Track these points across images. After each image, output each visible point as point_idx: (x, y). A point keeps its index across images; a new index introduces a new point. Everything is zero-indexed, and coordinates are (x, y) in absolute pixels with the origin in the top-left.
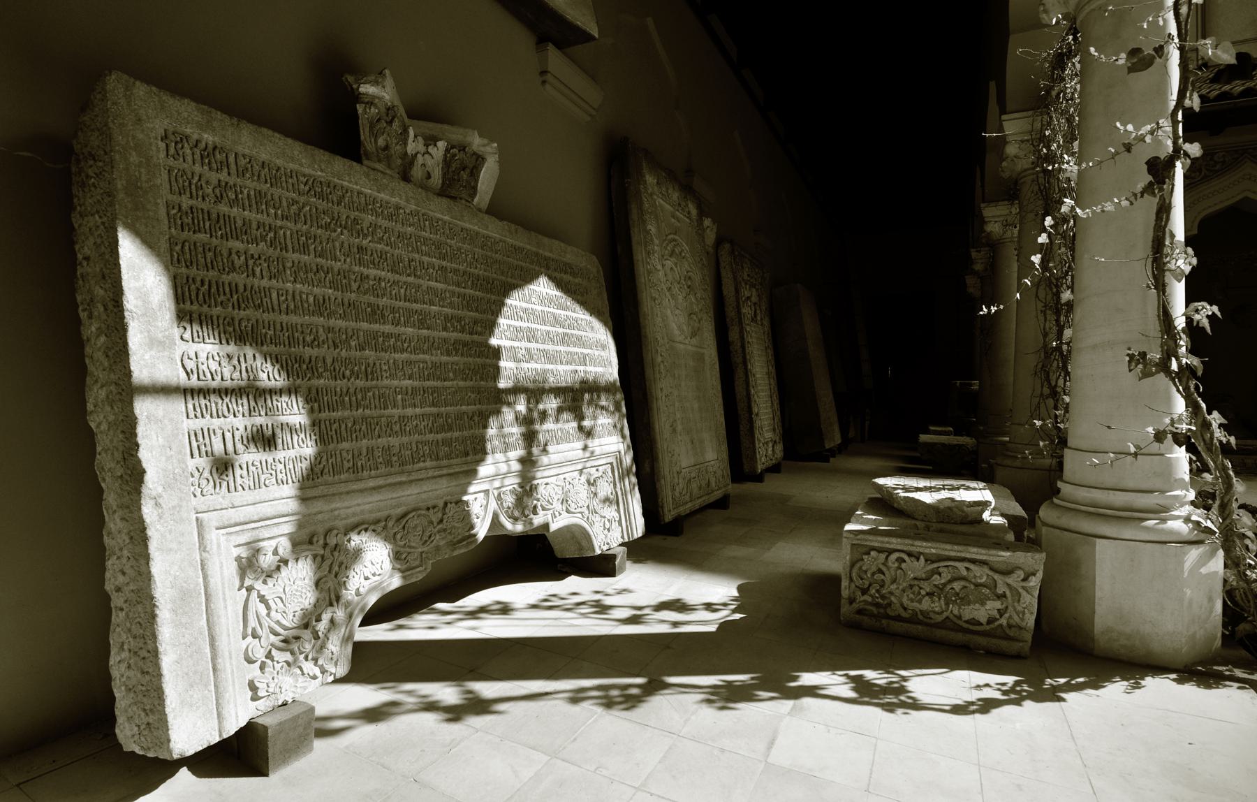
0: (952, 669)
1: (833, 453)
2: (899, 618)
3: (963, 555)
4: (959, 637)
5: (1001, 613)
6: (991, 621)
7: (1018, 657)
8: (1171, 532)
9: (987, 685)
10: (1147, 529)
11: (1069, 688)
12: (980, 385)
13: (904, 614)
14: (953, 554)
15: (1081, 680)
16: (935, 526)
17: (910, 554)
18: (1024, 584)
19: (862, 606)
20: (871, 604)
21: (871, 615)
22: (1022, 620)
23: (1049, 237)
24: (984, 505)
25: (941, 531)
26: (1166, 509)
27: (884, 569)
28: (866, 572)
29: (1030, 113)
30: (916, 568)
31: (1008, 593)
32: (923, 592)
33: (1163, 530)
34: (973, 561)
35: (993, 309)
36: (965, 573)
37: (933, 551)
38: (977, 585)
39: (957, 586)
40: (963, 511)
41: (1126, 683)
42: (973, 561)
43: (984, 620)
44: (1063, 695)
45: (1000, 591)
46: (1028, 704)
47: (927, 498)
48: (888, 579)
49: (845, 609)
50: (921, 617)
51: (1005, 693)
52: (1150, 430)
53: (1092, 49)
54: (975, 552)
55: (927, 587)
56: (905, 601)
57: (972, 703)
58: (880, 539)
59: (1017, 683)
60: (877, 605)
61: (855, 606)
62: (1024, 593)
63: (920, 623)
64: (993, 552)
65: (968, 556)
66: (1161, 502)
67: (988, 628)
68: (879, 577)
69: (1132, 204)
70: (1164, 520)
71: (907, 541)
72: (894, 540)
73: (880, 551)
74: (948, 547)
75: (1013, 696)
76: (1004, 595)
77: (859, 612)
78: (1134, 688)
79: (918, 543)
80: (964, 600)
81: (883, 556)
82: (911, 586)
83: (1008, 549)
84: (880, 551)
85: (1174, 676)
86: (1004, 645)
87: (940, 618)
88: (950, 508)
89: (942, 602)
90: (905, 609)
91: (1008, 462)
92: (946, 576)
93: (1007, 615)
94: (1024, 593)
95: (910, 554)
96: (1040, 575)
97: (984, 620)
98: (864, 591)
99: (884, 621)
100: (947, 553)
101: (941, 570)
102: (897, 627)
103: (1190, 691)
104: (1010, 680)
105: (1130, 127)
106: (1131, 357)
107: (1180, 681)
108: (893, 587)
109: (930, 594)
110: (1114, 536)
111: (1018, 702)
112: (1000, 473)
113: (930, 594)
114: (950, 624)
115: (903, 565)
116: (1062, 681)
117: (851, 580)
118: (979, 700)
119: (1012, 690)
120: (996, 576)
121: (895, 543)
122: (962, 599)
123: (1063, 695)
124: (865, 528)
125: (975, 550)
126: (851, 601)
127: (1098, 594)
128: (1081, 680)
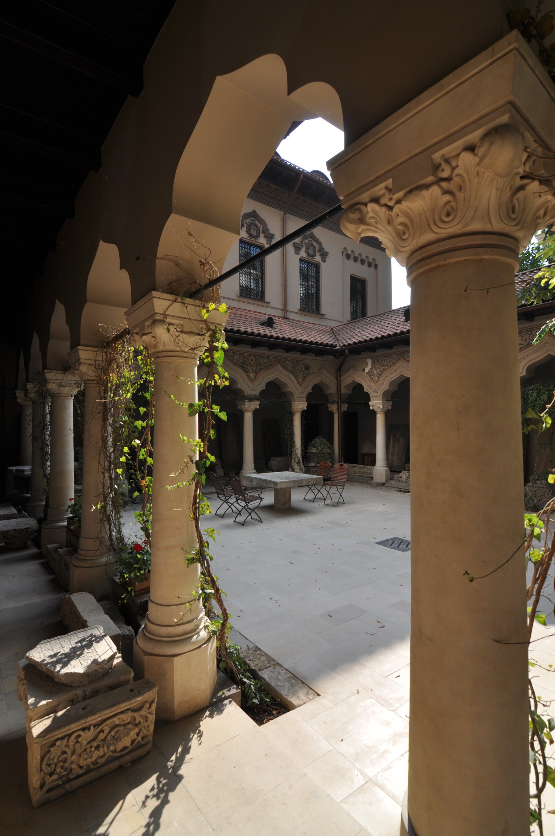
0: (124, 797)
2: (79, 776)
3: (117, 712)
4: (117, 763)
5: (138, 734)
6: (133, 742)
7: (148, 753)
8: (202, 640)
9: (147, 797)
10: (194, 643)
11: (180, 761)
12: (32, 470)
13: (81, 772)
14: (111, 714)
15: (180, 750)
16: (89, 689)
17: (83, 729)
18: (150, 710)
19: (50, 785)
20: (58, 779)
21: (58, 786)
22: (148, 731)
23: (127, 459)
24: (112, 657)
25: (96, 693)
26: (197, 626)
27: (66, 749)
28: (53, 759)
29: (96, 349)
31: (142, 721)
32: (93, 749)
33: (199, 640)
34: (122, 713)
35: (99, 506)
36: (117, 722)
37: (99, 719)
38: (124, 725)
40: (104, 669)
41: (196, 736)
42: (122, 713)
43: (128, 745)
44: (180, 772)
45: (137, 722)
46: (172, 796)
47: (78, 667)
48: (69, 753)
49: (36, 796)
50: (92, 767)
51: (157, 796)
52: (194, 592)
53: (172, 396)
54: (124, 706)
55: (95, 744)
56: (82, 762)
57: (148, 825)
58: (63, 730)
59: (158, 779)
61: (45, 788)
62: (148, 715)
64: (133, 701)
65: (120, 711)
66: (196, 624)
67: (131, 747)
69: (190, 484)
70: (198, 633)
71: (83, 721)
72: (73, 726)
73: (62, 738)
74: (108, 711)
75: (162, 796)
76: (139, 723)
77: (49, 791)
78: (200, 736)
79: (89, 719)
80: (116, 739)
81: (65, 741)
82: (85, 751)
83: (140, 694)
84: (62, 738)
85: (207, 713)
86: (140, 752)
87: (103, 760)
88: (96, 670)
89: (105, 748)
90: (81, 767)
91: (82, 564)
92: (106, 731)
93: (141, 734)
94: (148, 715)
95: (83, 729)
96: (156, 701)
97: (128, 745)
98: (51, 774)
99: (67, 786)
100: (108, 716)
101: (104, 729)
102: (76, 784)
103: (216, 718)
104: (152, 781)
105: (185, 438)
106: (188, 560)
107: (211, 716)
108: (74, 758)
109: (97, 748)
110: (181, 652)
111: (165, 802)
112: (77, 574)
115: (80, 739)
116: (173, 758)
117: (41, 770)
118: (150, 817)
119: (160, 791)
120: (136, 714)
121: (74, 727)
122: (116, 739)
123: (180, 772)
124: (47, 722)
125: (123, 705)
126: (42, 787)
127: (176, 686)
128: (180, 750)
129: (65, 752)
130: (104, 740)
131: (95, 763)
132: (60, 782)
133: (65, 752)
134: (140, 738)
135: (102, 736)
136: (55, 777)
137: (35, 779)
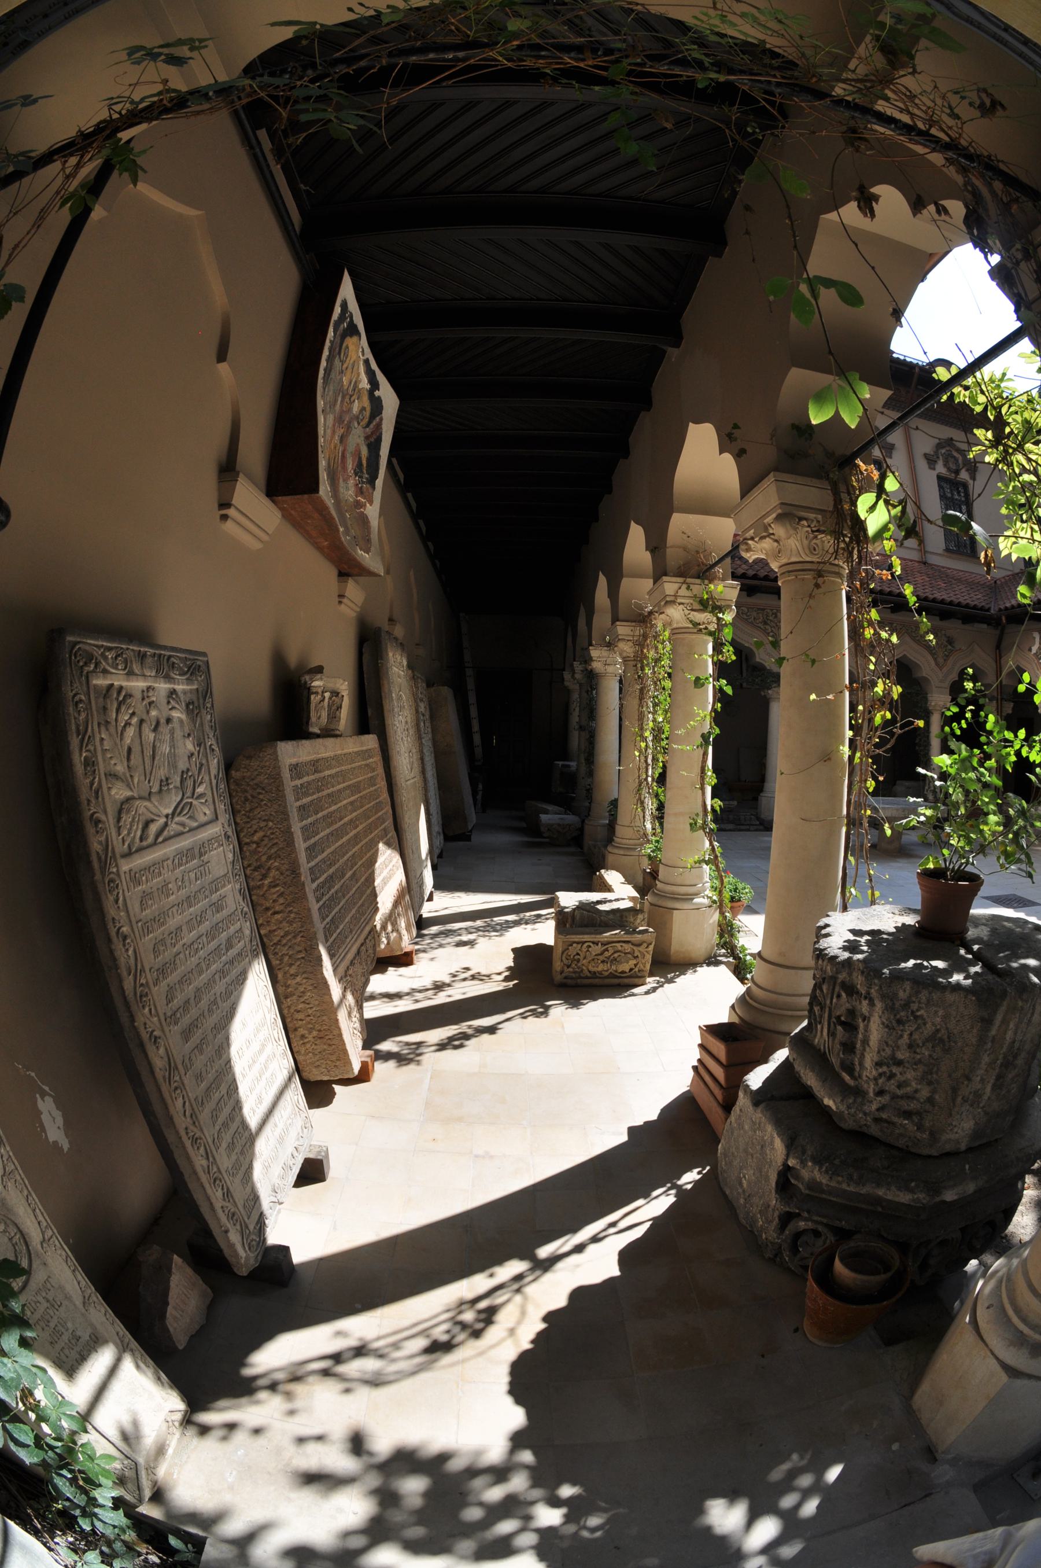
1: (471, 831)
2: (587, 978)
6: (631, 970)
17: (593, 943)
21: (572, 978)
30: (596, 949)
39: (616, 955)
42: (624, 942)
49: (558, 978)
55: (601, 958)
56: (590, 968)
60: (575, 972)
61: (564, 975)
63: (597, 977)
68: (577, 957)
73: (578, 943)
77: (566, 978)
84: (578, 943)
87: (606, 974)
92: (611, 951)
95: (593, 943)
98: (568, 967)
113: (603, 962)
114: (612, 976)
126: (562, 972)
129: (578, 954)
130: (608, 958)
131: (600, 973)
132: (574, 975)
133: (578, 954)
134: (637, 969)
135: (607, 954)
136: (571, 970)
137: (557, 965)
